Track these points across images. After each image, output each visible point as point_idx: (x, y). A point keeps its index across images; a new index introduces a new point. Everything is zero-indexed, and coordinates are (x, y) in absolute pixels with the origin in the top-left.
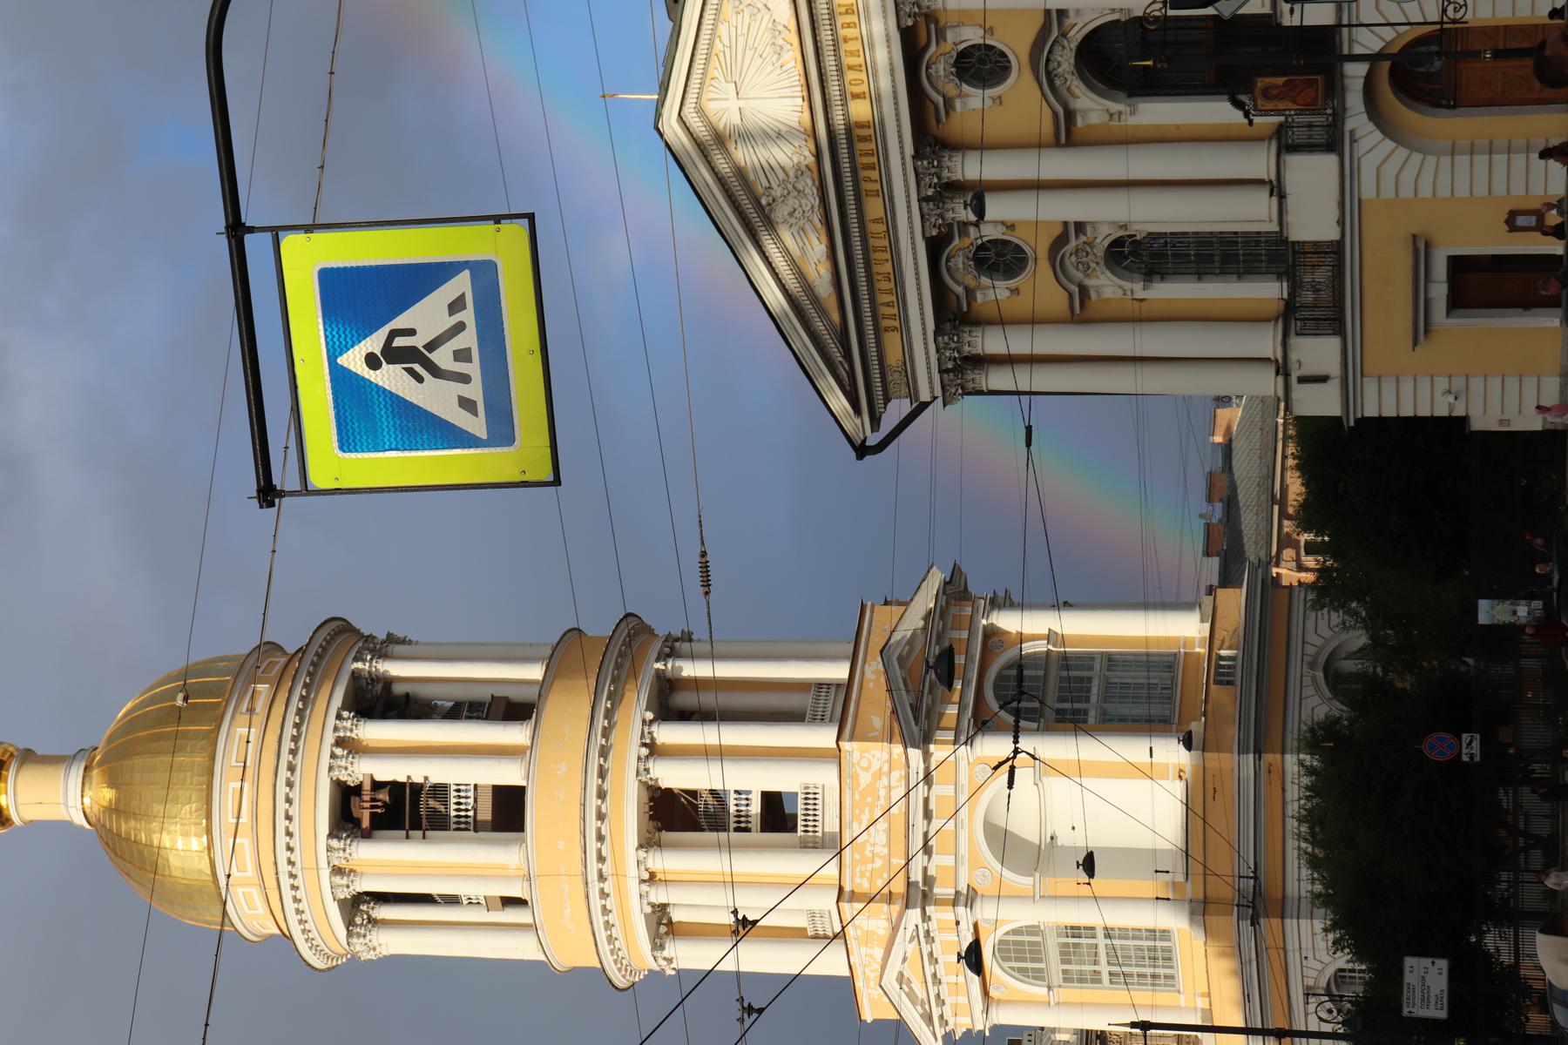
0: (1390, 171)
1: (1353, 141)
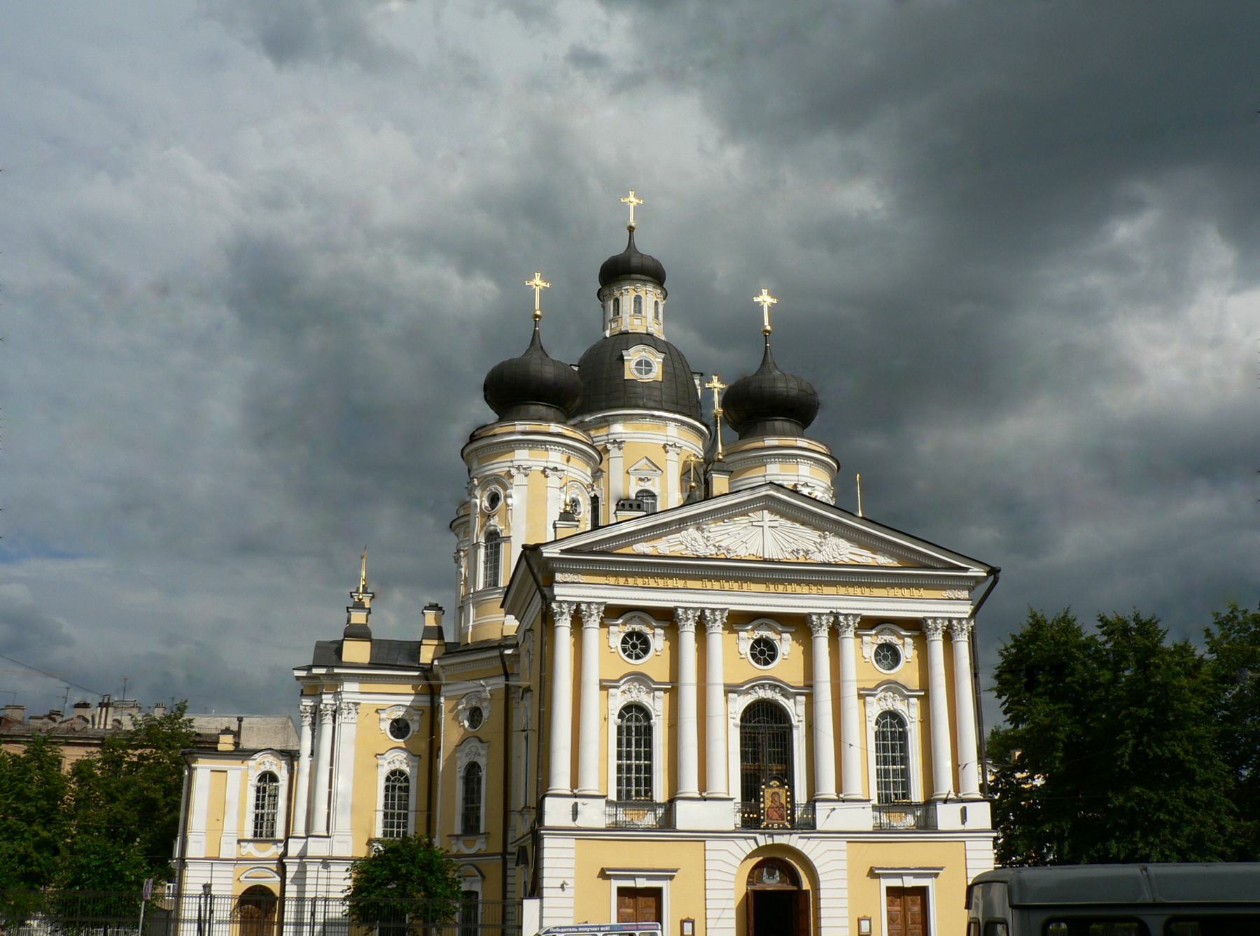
0: (724, 856)
1: (746, 838)
